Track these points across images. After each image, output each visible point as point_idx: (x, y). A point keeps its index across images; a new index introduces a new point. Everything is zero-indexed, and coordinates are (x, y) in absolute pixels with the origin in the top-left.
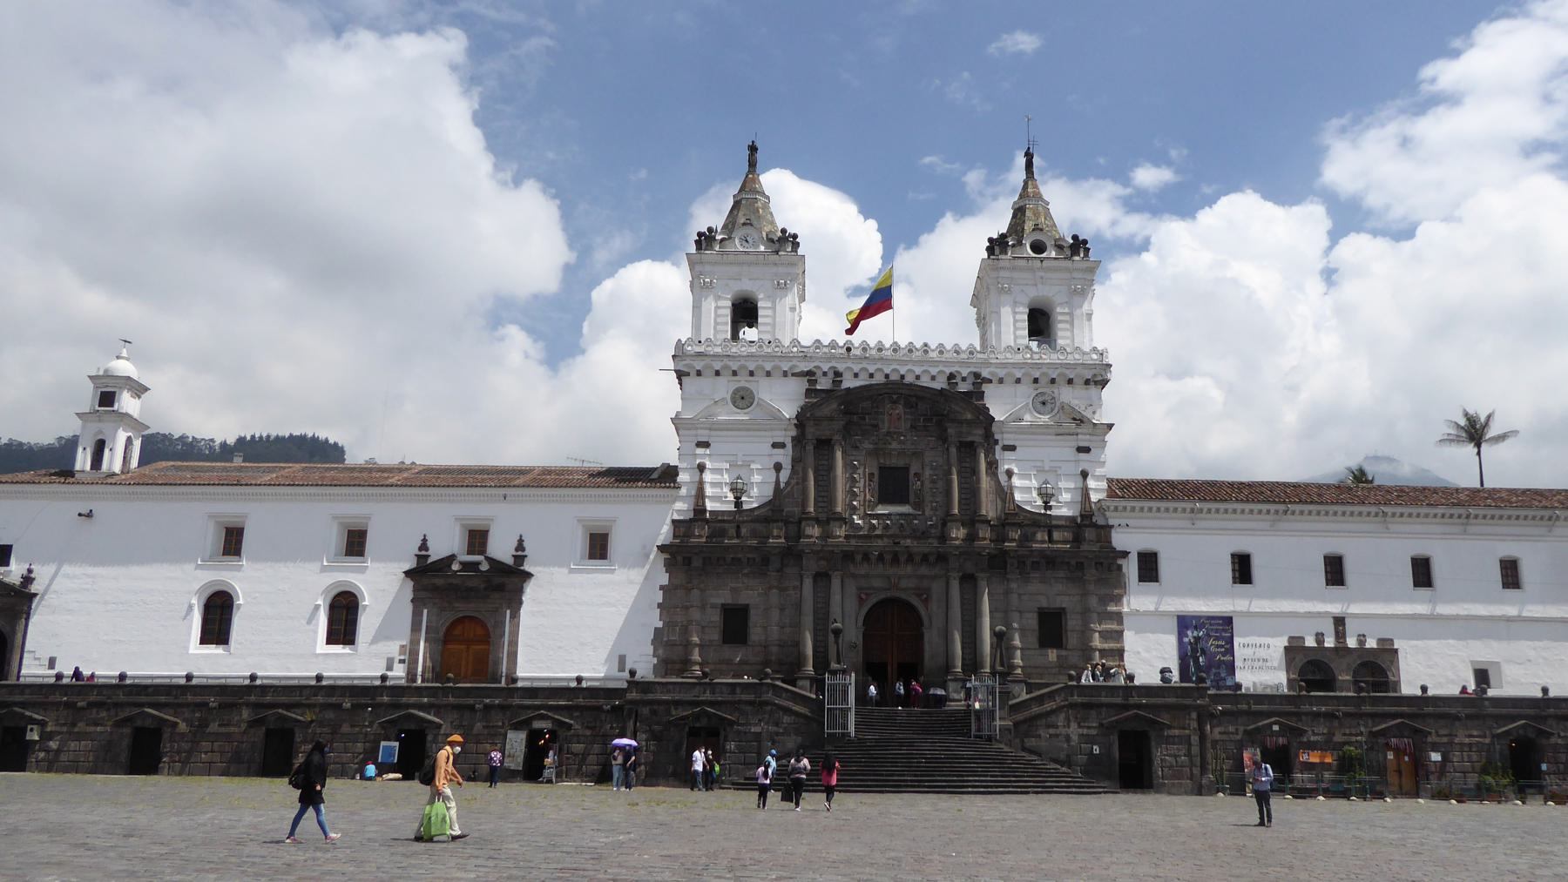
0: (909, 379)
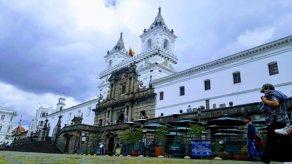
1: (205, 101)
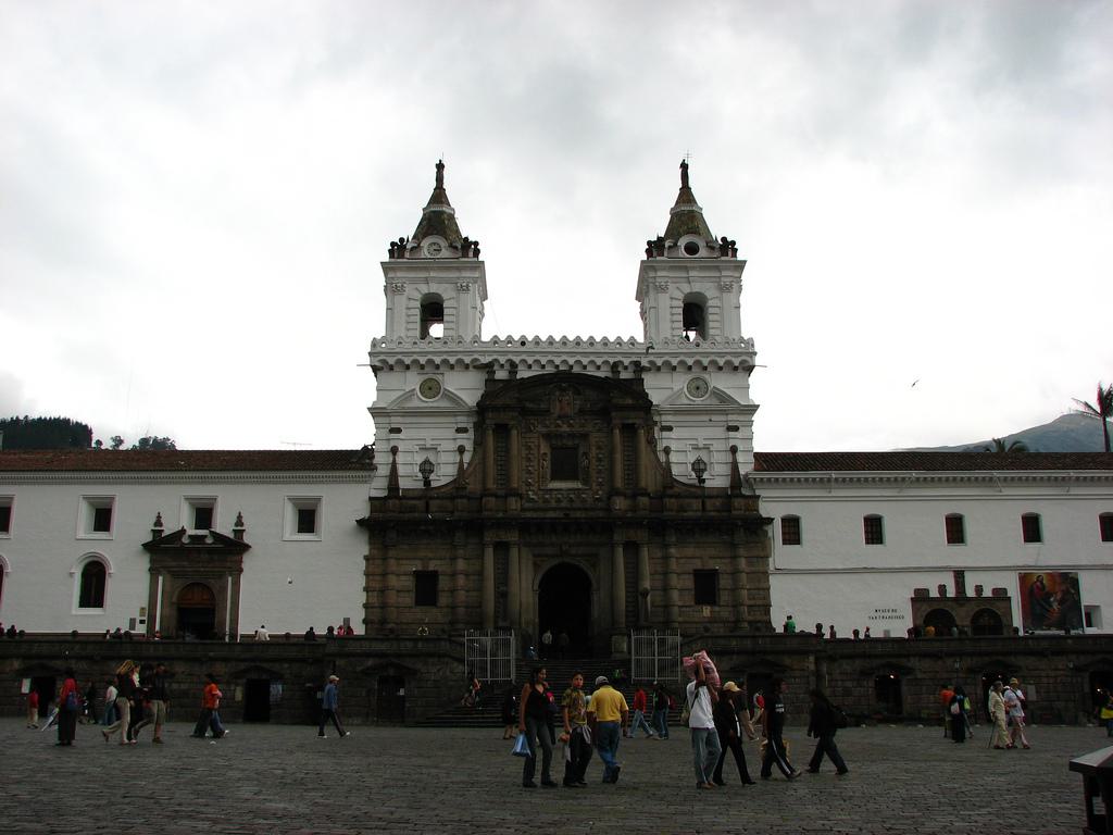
0: (576, 369)
1: (952, 574)
